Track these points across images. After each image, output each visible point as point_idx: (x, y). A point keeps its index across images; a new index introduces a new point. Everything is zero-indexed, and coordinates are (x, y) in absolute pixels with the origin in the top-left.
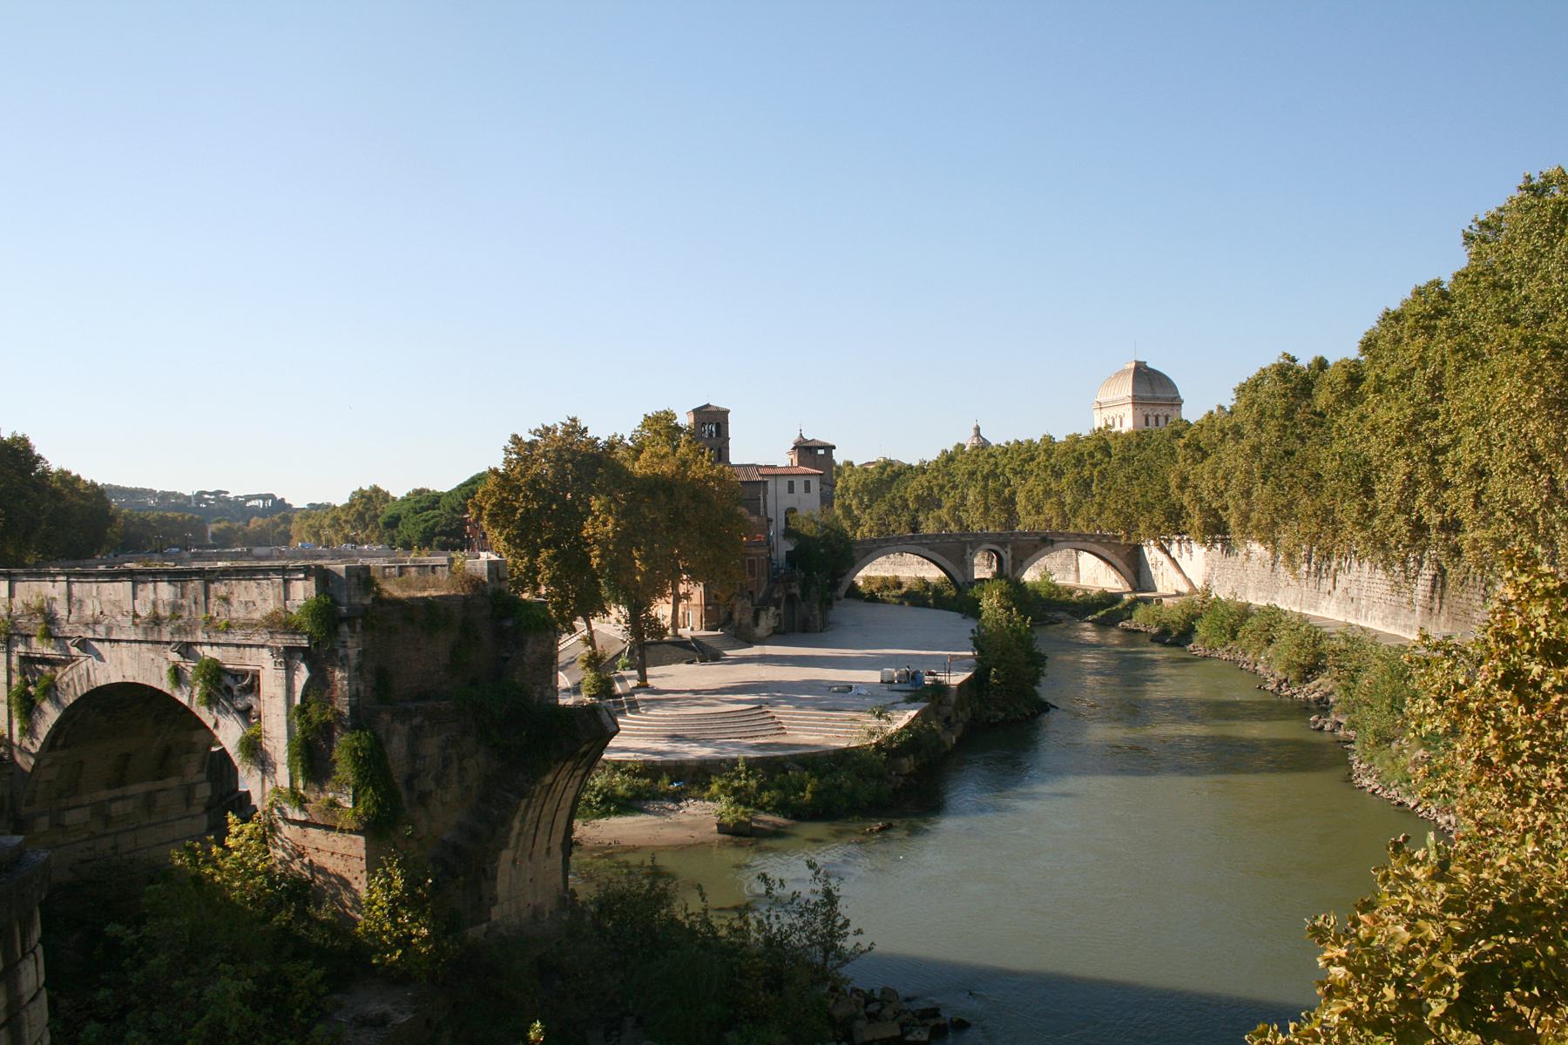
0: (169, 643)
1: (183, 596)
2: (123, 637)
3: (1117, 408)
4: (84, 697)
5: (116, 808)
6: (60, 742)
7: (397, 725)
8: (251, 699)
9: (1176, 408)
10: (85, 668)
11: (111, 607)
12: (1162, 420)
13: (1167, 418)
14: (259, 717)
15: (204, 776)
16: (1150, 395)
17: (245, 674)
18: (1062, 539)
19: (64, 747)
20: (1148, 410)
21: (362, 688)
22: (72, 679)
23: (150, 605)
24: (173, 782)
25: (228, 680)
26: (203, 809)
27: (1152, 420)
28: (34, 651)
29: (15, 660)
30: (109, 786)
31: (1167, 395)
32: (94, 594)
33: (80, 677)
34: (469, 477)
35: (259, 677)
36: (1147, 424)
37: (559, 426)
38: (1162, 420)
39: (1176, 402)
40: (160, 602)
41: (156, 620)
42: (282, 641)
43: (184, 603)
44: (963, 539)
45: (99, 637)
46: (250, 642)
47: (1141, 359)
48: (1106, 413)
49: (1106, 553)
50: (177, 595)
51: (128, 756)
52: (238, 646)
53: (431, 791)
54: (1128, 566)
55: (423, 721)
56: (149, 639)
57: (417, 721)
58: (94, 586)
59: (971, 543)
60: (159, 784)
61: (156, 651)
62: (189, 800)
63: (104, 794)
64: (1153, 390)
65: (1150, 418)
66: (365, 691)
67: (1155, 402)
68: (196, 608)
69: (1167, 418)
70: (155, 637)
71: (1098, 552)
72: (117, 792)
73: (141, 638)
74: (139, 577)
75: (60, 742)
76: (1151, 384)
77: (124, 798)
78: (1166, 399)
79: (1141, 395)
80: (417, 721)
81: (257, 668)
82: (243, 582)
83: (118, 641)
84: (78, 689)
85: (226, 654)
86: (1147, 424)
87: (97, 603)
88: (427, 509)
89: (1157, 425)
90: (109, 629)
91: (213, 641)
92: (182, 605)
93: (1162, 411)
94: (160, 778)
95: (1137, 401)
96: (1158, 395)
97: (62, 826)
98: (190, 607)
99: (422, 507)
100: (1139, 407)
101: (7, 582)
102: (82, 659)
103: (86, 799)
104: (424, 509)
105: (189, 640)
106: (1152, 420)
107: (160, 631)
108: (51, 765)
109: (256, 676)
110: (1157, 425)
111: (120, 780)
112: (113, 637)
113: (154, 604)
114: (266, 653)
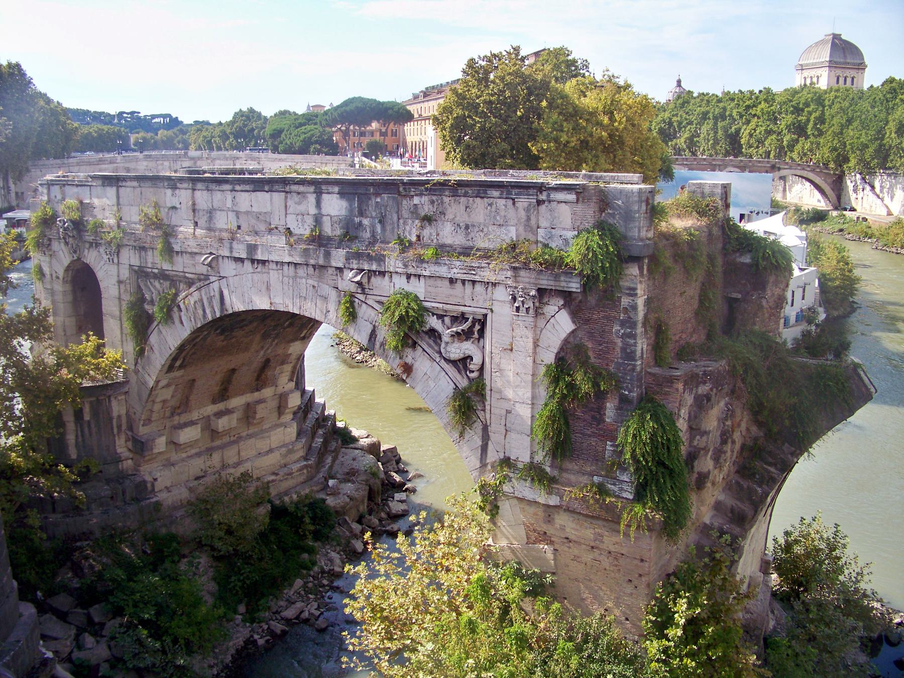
0: (340, 270)
1: (361, 214)
2: (271, 258)
3: (816, 70)
4: (215, 321)
5: (222, 424)
6: (178, 364)
7: (686, 395)
8: (467, 347)
9: (860, 71)
10: (217, 290)
11: (253, 221)
12: (849, 80)
13: (853, 79)
14: (481, 369)
15: (292, 385)
16: (842, 60)
17: (460, 318)
18: (786, 167)
19: (181, 367)
20: (839, 72)
21: (645, 346)
22: (201, 300)
23: (310, 221)
24: (267, 392)
25: (433, 322)
26: (291, 416)
27: (841, 80)
28: (150, 265)
29: (125, 273)
30: (214, 402)
31: (855, 61)
32: (229, 204)
33: (210, 299)
34: (391, 99)
35: (483, 324)
36: (838, 82)
37: (504, 53)
38: (849, 80)
39: (861, 66)
40: (326, 220)
41: (319, 240)
42: (528, 281)
43: (366, 222)
44: (714, 163)
45: (237, 255)
46: (477, 278)
47: (837, 32)
48: (806, 73)
49: (818, 180)
50: (351, 210)
51: (233, 371)
52: (452, 281)
53: (709, 472)
54: (833, 190)
55: (711, 389)
56: (312, 262)
57: (703, 389)
58: (229, 196)
59: (719, 165)
60: (257, 395)
61: (320, 278)
62: (281, 409)
63: (211, 409)
64: (845, 57)
65: (840, 79)
66: (647, 350)
67: (844, 66)
68: (384, 229)
69: (853, 79)
70: (321, 262)
71: (813, 180)
72: (221, 406)
73: (297, 259)
74: (295, 188)
75: (178, 364)
76: (844, 52)
77: (228, 412)
78: (854, 64)
79: (835, 60)
80: (703, 389)
81: (484, 311)
82: (463, 199)
83: (264, 262)
84: (208, 311)
85: (430, 289)
86: (838, 82)
87: (232, 216)
88: (304, 124)
89: (845, 83)
90: (252, 248)
91: (411, 271)
92: (360, 224)
93: (850, 73)
94: (258, 390)
95: (832, 65)
96: (848, 61)
97: (175, 443)
98: (373, 226)
99: (300, 123)
100: (833, 69)
101: (114, 189)
102: (212, 279)
103: (195, 416)
104: (301, 125)
105: (374, 267)
106: (841, 80)
107: (328, 255)
108: (168, 386)
109: (482, 322)
110: (845, 83)
111: (223, 394)
112: (259, 256)
113: (318, 220)
114: (502, 294)
